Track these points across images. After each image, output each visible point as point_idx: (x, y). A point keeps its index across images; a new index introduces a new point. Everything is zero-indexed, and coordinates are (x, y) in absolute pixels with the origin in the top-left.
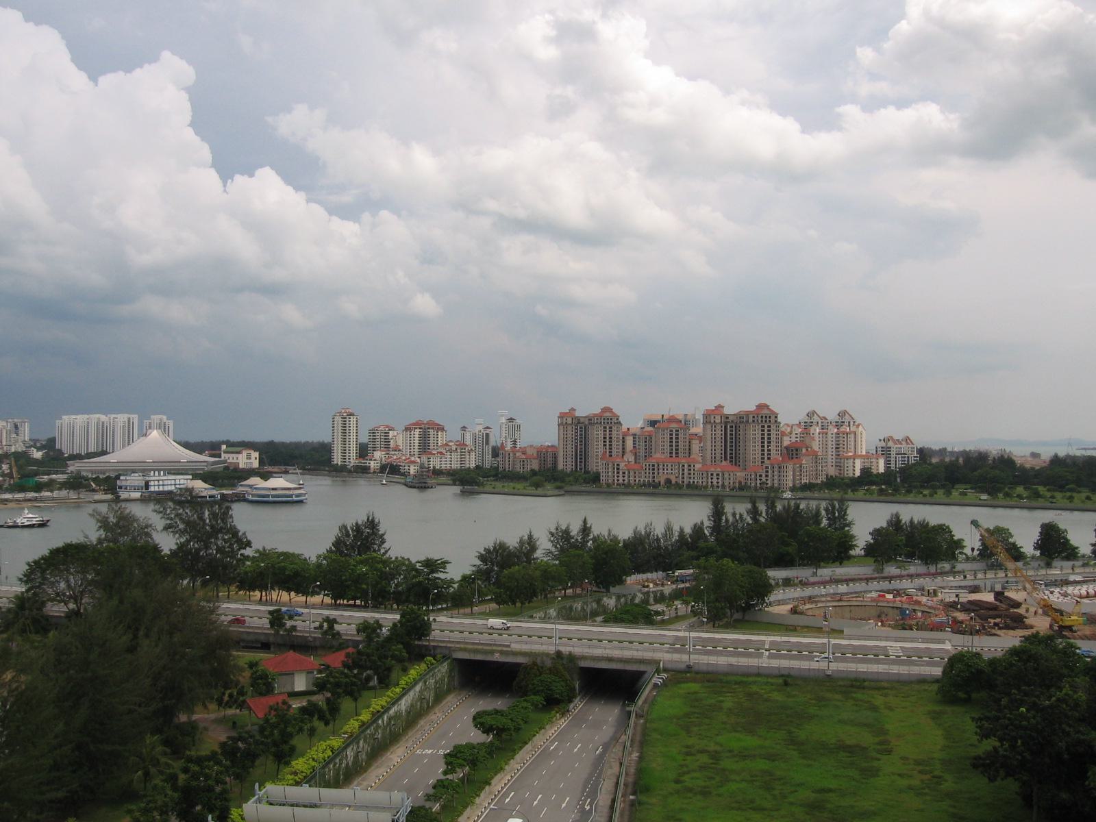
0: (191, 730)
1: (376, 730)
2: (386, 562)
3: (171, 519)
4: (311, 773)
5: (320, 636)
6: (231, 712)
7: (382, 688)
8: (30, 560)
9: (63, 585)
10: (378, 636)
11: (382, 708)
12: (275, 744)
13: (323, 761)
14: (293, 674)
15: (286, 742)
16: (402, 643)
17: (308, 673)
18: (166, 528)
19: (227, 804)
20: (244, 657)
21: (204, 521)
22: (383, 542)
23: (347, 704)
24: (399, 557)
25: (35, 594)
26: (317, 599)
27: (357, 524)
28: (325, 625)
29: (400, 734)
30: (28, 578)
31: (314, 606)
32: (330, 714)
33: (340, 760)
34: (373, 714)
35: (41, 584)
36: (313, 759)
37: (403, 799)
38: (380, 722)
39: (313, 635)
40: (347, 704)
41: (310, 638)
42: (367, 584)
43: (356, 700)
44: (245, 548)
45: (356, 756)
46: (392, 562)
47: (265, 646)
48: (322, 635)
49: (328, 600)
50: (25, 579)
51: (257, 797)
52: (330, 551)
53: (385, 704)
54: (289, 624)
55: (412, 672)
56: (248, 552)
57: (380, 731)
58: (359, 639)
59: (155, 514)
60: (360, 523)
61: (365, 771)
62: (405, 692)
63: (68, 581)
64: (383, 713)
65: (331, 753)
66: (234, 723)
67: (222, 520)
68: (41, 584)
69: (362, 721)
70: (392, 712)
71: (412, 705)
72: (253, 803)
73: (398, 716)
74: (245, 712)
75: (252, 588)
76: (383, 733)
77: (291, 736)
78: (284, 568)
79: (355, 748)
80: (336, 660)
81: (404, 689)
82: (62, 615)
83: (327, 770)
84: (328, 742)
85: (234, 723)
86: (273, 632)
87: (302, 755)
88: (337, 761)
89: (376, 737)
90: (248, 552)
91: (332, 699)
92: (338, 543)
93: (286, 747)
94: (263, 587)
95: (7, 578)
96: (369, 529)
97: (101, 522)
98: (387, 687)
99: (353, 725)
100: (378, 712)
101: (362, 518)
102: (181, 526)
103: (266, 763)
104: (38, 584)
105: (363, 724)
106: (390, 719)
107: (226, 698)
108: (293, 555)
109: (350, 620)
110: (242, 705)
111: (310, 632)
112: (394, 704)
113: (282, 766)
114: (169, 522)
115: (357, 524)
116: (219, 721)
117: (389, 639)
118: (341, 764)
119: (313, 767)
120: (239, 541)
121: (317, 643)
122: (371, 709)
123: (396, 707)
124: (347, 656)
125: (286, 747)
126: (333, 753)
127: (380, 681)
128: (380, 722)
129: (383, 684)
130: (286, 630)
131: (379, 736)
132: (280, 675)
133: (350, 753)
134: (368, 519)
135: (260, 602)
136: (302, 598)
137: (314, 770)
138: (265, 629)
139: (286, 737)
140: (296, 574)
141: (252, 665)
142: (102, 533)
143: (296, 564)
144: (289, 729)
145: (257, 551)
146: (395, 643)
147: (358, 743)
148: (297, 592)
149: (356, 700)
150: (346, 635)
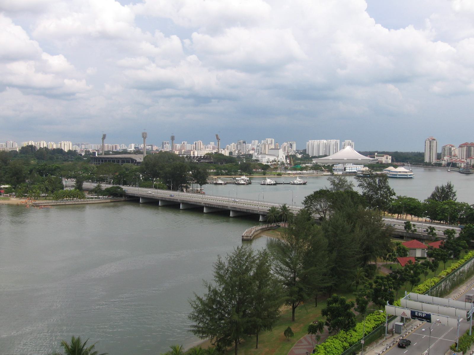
0: (373, 267)
1: (454, 277)
2: (456, 204)
3: (361, 182)
4: (426, 291)
5: (427, 235)
6: (389, 262)
7: (456, 259)
8: (306, 196)
9: (318, 207)
10: (453, 236)
11: (456, 268)
12: (412, 277)
13: (431, 287)
14: (416, 249)
15: (416, 277)
16: (466, 240)
17: (422, 249)
18: (360, 185)
19: (393, 298)
20: (395, 241)
21: (376, 183)
22: (455, 195)
23: (441, 264)
24: (463, 202)
25: (308, 210)
26: (424, 219)
27: (443, 187)
28: (429, 230)
29: (464, 280)
30: (306, 202)
31: (421, 222)
32: (434, 267)
33: (438, 287)
34: (452, 270)
35: (310, 205)
36: (427, 285)
37: (472, 306)
38: (456, 273)
39: (423, 234)
40: (441, 264)
41: (422, 235)
42: (448, 214)
43: (445, 262)
44: (392, 196)
45: (445, 287)
46: (460, 205)
47: (401, 237)
48: (428, 234)
49: (428, 219)
50: (304, 203)
51: (405, 297)
52: (429, 199)
53: (458, 266)
54: (413, 228)
55: (470, 253)
56: (394, 197)
57: (455, 277)
58: (444, 237)
59: (355, 179)
60: (444, 186)
61: (449, 294)
62: (467, 262)
63: (321, 205)
64: (457, 270)
65: (434, 284)
66: (391, 267)
67: (384, 183)
68: (310, 205)
69: (447, 272)
70: (461, 270)
71: (470, 268)
72: (404, 299)
73: (463, 272)
74: (396, 263)
75: (395, 212)
76: (457, 278)
77: (419, 274)
78: (410, 205)
79: (445, 283)
80: (436, 245)
81: (466, 261)
82: (317, 218)
83: (433, 290)
84: (433, 279)
85: (391, 267)
86: (406, 232)
87: (422, 283)
88: (437, 287)
89: (454, 280)
90: (394, 197)
91: (435, 261)
92: (433, 195)
93: (416, 279)
94: (399, 213)
95: (295, 203)
96: (448, 189)
97: (332, 182)
98: (458, 259)
99: (443, 274)
100: (455, 269)
101: (445, 184)
102: (366, 185)
103: (408, 284)
104: (309, 205)
105: (448, 274)
106: (460, 273)
107: (387, 256)
108: (414, 199)
109: (440, 229)
110: (394, 260)
111: (422, 233)
112: (462, 267)
113: (414, 286)
114: (360, 183)
115: (443, 187)
116: (385, 266)
117: (459, 238)
118: (439, 289)
119: (427, 289)
120: (390, 192)
121: (425, 238)
122: (451, 267)
123: (463, 267)
124: (442, 243)
125: (416, 279)
126: (435, 284)
127: (455, 257)
128: (456, 273)
129: (456, 257)
130: (412, 231)
131: (455, 280)
132: (410, 249)
133: (443, 285)
134: (448, 185)
135: (397, 219)
136: (416, 218)
137: (427, 290)
138: (402, 230)
139: (416, 274)
140: (415, 207)
141: (398, 244)
142: (332, 186)
143: (415, 203)
144: (418, 271)
145: (397, 197)
146: (462, 240)
147: (446, 281)
148: (415, 215)
149: (445, 262)
150: (438, 235)
